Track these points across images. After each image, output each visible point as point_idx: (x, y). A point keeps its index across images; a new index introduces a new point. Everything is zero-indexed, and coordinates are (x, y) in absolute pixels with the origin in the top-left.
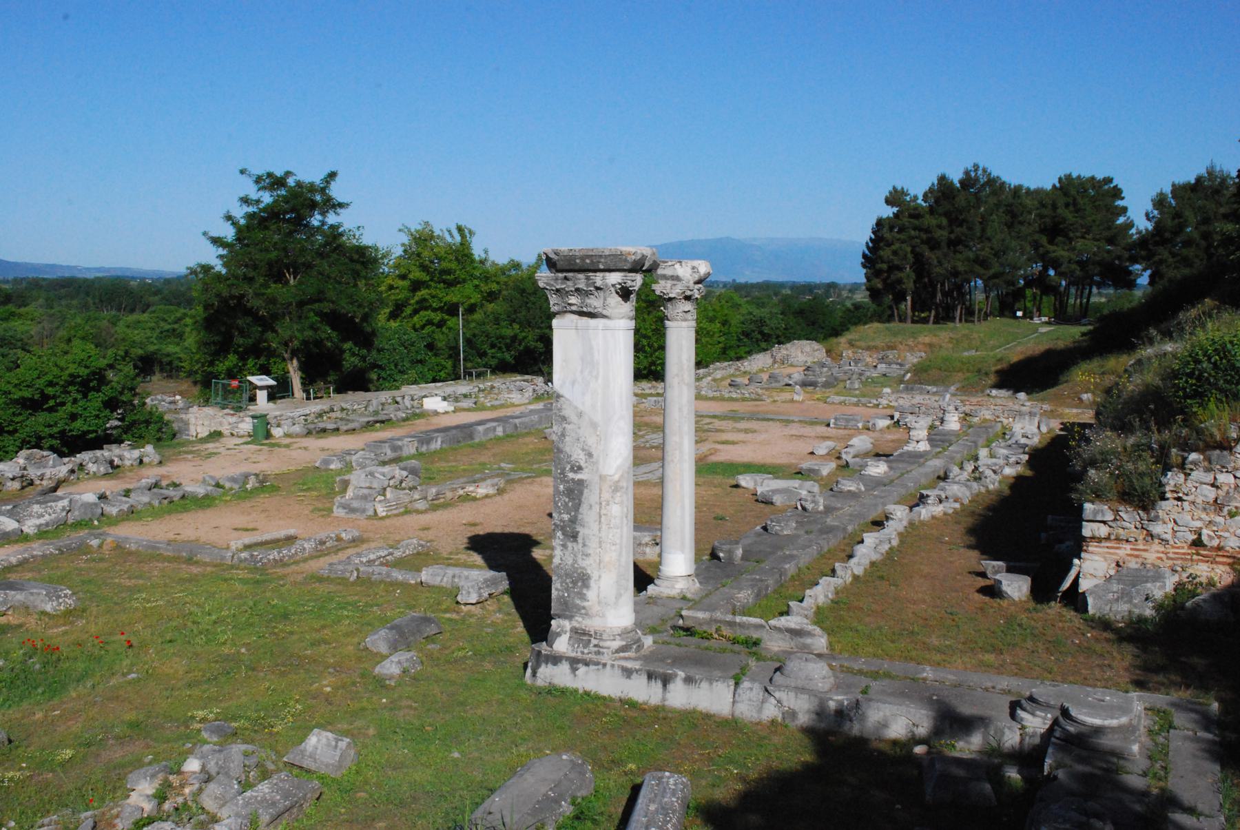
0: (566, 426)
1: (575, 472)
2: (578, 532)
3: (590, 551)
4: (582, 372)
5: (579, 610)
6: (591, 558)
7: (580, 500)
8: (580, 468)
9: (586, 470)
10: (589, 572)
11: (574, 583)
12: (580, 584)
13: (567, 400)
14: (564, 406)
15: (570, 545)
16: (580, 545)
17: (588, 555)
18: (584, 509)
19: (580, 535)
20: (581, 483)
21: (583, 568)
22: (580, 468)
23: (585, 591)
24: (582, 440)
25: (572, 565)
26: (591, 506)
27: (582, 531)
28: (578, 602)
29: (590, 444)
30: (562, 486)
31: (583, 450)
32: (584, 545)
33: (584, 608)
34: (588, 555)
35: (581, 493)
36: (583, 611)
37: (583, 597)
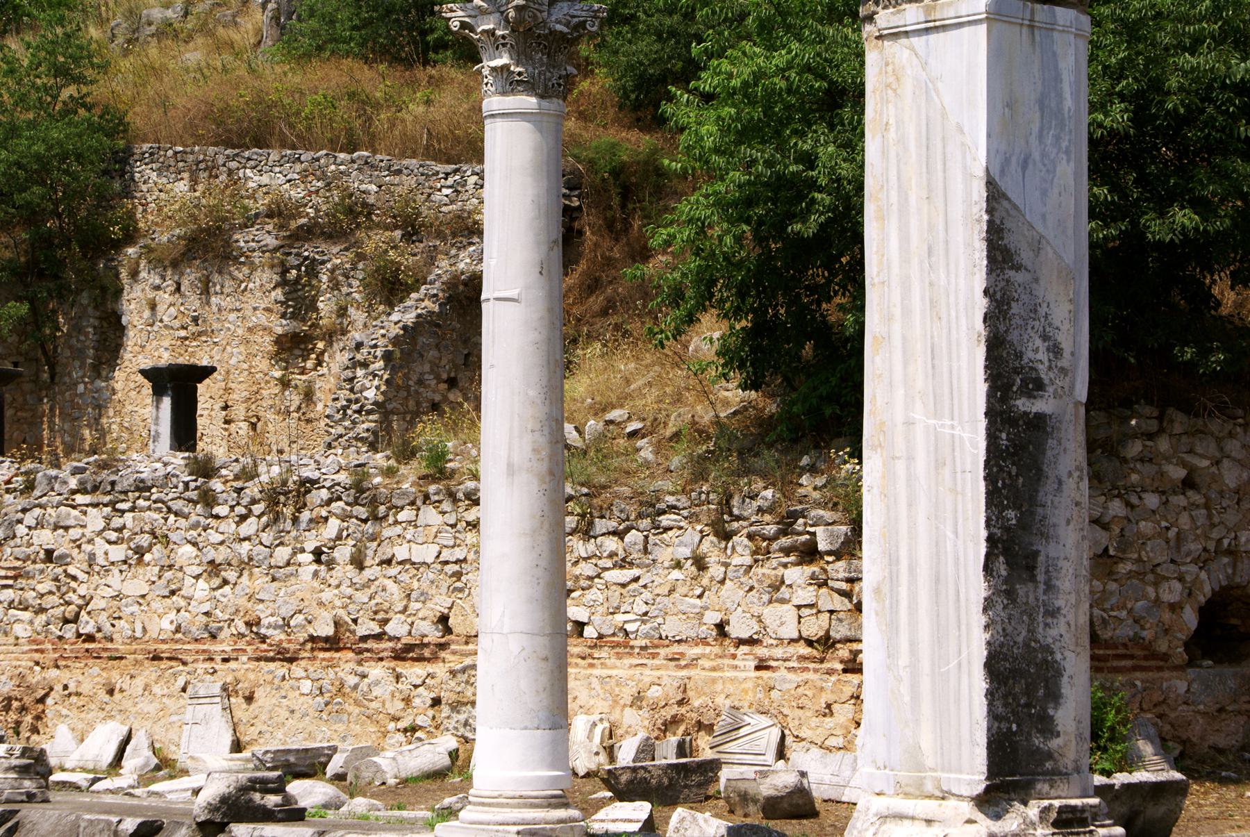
0: (1011, 274)
1: (1030, 396)
2: (1037, 553)
3: (1060, 603)
4: (1041, 137)
5: (1041, 763)
6: (1062, 621)
7: (1039, 471)
8: (1039, 385)
9: (1051, 389)
10: (1058, 657)
11: (1029, 691)
12: (1041, 692)
13: (1015, 207)
14: (1008, 225)
15: (1021, 590)
16: (1042, 587)
17: (1053, 613)
18: (1046, 493)
19: (1041, 558)
20: (1038, 423)
21: (1048, 649)
22: (1039, 385)
23: (1051, 712)
24: (1042, 310)
25: (1026, 645)
26: (1060, 483)
27: (1048, 551)
28: (1037, 741)
29: (1057, 323)
30: (1004, 436)
31: (1045, 337)
32: (1049, 587)
33: (1049, 755)
34: (1053, 613)
35: (1041, 449)
36: (1049, 765)
37: (1047, 727)
